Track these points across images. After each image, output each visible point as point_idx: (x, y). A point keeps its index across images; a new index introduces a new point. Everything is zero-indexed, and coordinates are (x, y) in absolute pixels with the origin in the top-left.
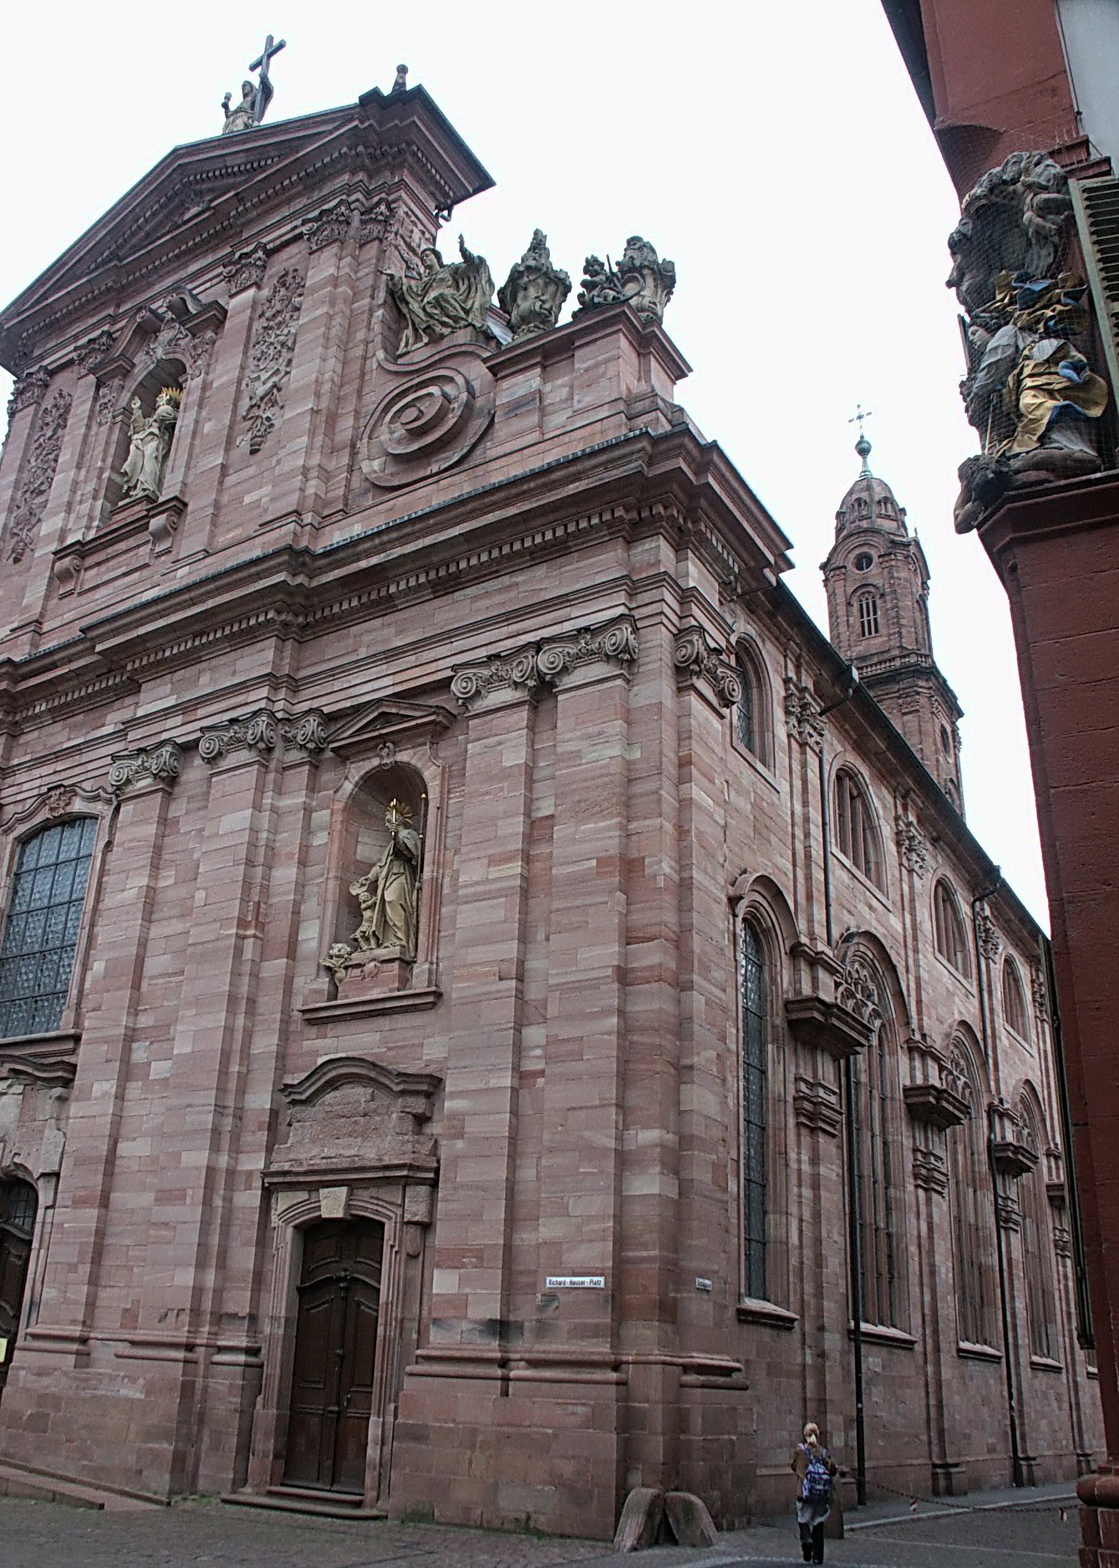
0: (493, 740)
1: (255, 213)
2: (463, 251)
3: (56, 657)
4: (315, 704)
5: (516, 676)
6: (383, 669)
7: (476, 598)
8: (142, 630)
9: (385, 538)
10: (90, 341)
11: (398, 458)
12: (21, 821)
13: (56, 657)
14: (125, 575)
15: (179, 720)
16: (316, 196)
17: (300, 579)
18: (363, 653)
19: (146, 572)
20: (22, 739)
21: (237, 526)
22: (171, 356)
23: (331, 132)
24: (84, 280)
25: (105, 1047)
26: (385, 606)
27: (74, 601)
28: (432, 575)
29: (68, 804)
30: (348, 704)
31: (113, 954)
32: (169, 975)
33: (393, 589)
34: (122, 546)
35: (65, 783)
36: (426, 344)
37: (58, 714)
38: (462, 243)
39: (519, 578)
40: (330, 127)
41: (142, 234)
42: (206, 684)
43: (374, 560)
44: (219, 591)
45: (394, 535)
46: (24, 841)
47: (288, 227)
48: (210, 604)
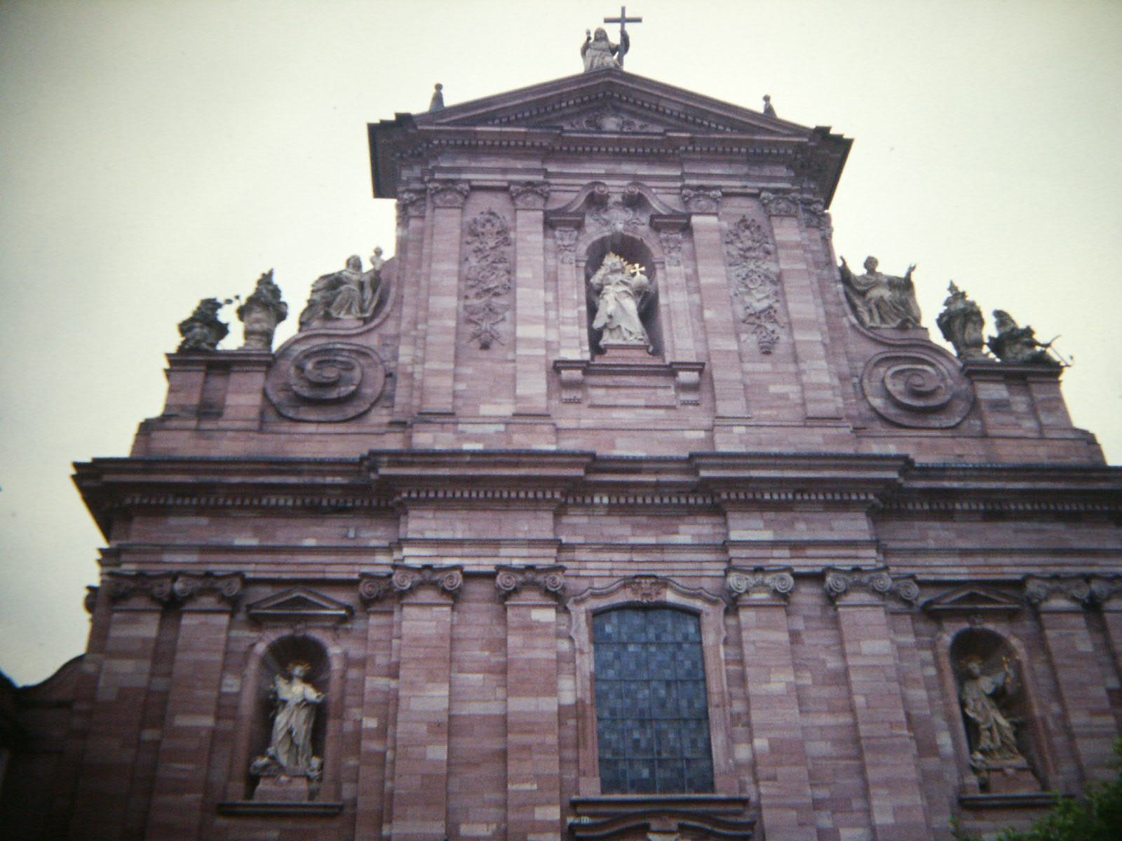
0: (1064, 631)
1: (699, 157)
2: (909, 274)
3: (645, 466)
4: (913, 571)
5: (1075, 593)
6: (957, 560)
7: (1016, 531)
8: (755, 473)
9: (968, 473)
10: (529, 183)
11: (898, 405)
12: (595, 596)
13: (645, 466)
14: (647, 407)
15: (786, 553)
16: (756, 171)
17: (901, 480)
18: (932, 544)
19: (672, 413)
20: (565, 520)
21: (771, 408)
22: (630, 234)
23: (788, 135)
24: (523, 130)
25: (794, 813)
26: (946, 515)
27: (584, 410)
28: (990, 507)
29: (658, 593)
30: (932, 578)
31: (772, 734)
32: (831, 758)
33: (958, 506)
34: (633, 380)
35: (659, 574)
36: (893, 328)
37: (612, 510)
38: (912, 269)
39: (1049, 527)
40: (786, 132)
41: (561, 114)
42: (801, 531)
43: (956, 485)
44: (836, 467)
45: (975, 473)
46: (596, 614)
47: (738, 184)
48: (826, 474)
